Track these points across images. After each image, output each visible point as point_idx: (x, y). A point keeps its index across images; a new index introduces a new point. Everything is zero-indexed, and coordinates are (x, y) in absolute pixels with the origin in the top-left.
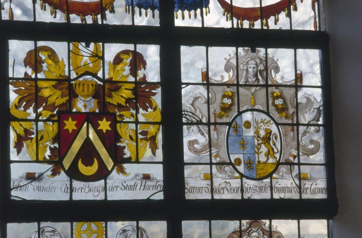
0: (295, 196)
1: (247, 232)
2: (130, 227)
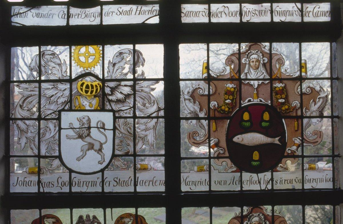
0: (297, 19)
1: (246, 55)
2: (127, 50)
